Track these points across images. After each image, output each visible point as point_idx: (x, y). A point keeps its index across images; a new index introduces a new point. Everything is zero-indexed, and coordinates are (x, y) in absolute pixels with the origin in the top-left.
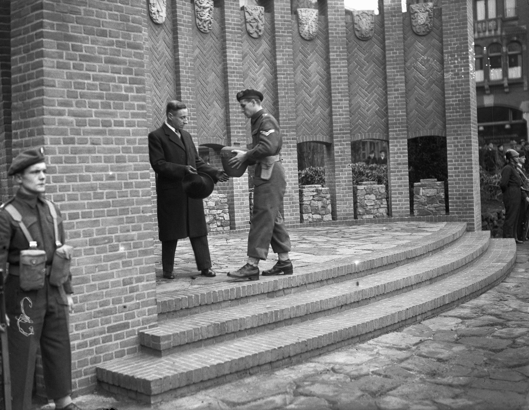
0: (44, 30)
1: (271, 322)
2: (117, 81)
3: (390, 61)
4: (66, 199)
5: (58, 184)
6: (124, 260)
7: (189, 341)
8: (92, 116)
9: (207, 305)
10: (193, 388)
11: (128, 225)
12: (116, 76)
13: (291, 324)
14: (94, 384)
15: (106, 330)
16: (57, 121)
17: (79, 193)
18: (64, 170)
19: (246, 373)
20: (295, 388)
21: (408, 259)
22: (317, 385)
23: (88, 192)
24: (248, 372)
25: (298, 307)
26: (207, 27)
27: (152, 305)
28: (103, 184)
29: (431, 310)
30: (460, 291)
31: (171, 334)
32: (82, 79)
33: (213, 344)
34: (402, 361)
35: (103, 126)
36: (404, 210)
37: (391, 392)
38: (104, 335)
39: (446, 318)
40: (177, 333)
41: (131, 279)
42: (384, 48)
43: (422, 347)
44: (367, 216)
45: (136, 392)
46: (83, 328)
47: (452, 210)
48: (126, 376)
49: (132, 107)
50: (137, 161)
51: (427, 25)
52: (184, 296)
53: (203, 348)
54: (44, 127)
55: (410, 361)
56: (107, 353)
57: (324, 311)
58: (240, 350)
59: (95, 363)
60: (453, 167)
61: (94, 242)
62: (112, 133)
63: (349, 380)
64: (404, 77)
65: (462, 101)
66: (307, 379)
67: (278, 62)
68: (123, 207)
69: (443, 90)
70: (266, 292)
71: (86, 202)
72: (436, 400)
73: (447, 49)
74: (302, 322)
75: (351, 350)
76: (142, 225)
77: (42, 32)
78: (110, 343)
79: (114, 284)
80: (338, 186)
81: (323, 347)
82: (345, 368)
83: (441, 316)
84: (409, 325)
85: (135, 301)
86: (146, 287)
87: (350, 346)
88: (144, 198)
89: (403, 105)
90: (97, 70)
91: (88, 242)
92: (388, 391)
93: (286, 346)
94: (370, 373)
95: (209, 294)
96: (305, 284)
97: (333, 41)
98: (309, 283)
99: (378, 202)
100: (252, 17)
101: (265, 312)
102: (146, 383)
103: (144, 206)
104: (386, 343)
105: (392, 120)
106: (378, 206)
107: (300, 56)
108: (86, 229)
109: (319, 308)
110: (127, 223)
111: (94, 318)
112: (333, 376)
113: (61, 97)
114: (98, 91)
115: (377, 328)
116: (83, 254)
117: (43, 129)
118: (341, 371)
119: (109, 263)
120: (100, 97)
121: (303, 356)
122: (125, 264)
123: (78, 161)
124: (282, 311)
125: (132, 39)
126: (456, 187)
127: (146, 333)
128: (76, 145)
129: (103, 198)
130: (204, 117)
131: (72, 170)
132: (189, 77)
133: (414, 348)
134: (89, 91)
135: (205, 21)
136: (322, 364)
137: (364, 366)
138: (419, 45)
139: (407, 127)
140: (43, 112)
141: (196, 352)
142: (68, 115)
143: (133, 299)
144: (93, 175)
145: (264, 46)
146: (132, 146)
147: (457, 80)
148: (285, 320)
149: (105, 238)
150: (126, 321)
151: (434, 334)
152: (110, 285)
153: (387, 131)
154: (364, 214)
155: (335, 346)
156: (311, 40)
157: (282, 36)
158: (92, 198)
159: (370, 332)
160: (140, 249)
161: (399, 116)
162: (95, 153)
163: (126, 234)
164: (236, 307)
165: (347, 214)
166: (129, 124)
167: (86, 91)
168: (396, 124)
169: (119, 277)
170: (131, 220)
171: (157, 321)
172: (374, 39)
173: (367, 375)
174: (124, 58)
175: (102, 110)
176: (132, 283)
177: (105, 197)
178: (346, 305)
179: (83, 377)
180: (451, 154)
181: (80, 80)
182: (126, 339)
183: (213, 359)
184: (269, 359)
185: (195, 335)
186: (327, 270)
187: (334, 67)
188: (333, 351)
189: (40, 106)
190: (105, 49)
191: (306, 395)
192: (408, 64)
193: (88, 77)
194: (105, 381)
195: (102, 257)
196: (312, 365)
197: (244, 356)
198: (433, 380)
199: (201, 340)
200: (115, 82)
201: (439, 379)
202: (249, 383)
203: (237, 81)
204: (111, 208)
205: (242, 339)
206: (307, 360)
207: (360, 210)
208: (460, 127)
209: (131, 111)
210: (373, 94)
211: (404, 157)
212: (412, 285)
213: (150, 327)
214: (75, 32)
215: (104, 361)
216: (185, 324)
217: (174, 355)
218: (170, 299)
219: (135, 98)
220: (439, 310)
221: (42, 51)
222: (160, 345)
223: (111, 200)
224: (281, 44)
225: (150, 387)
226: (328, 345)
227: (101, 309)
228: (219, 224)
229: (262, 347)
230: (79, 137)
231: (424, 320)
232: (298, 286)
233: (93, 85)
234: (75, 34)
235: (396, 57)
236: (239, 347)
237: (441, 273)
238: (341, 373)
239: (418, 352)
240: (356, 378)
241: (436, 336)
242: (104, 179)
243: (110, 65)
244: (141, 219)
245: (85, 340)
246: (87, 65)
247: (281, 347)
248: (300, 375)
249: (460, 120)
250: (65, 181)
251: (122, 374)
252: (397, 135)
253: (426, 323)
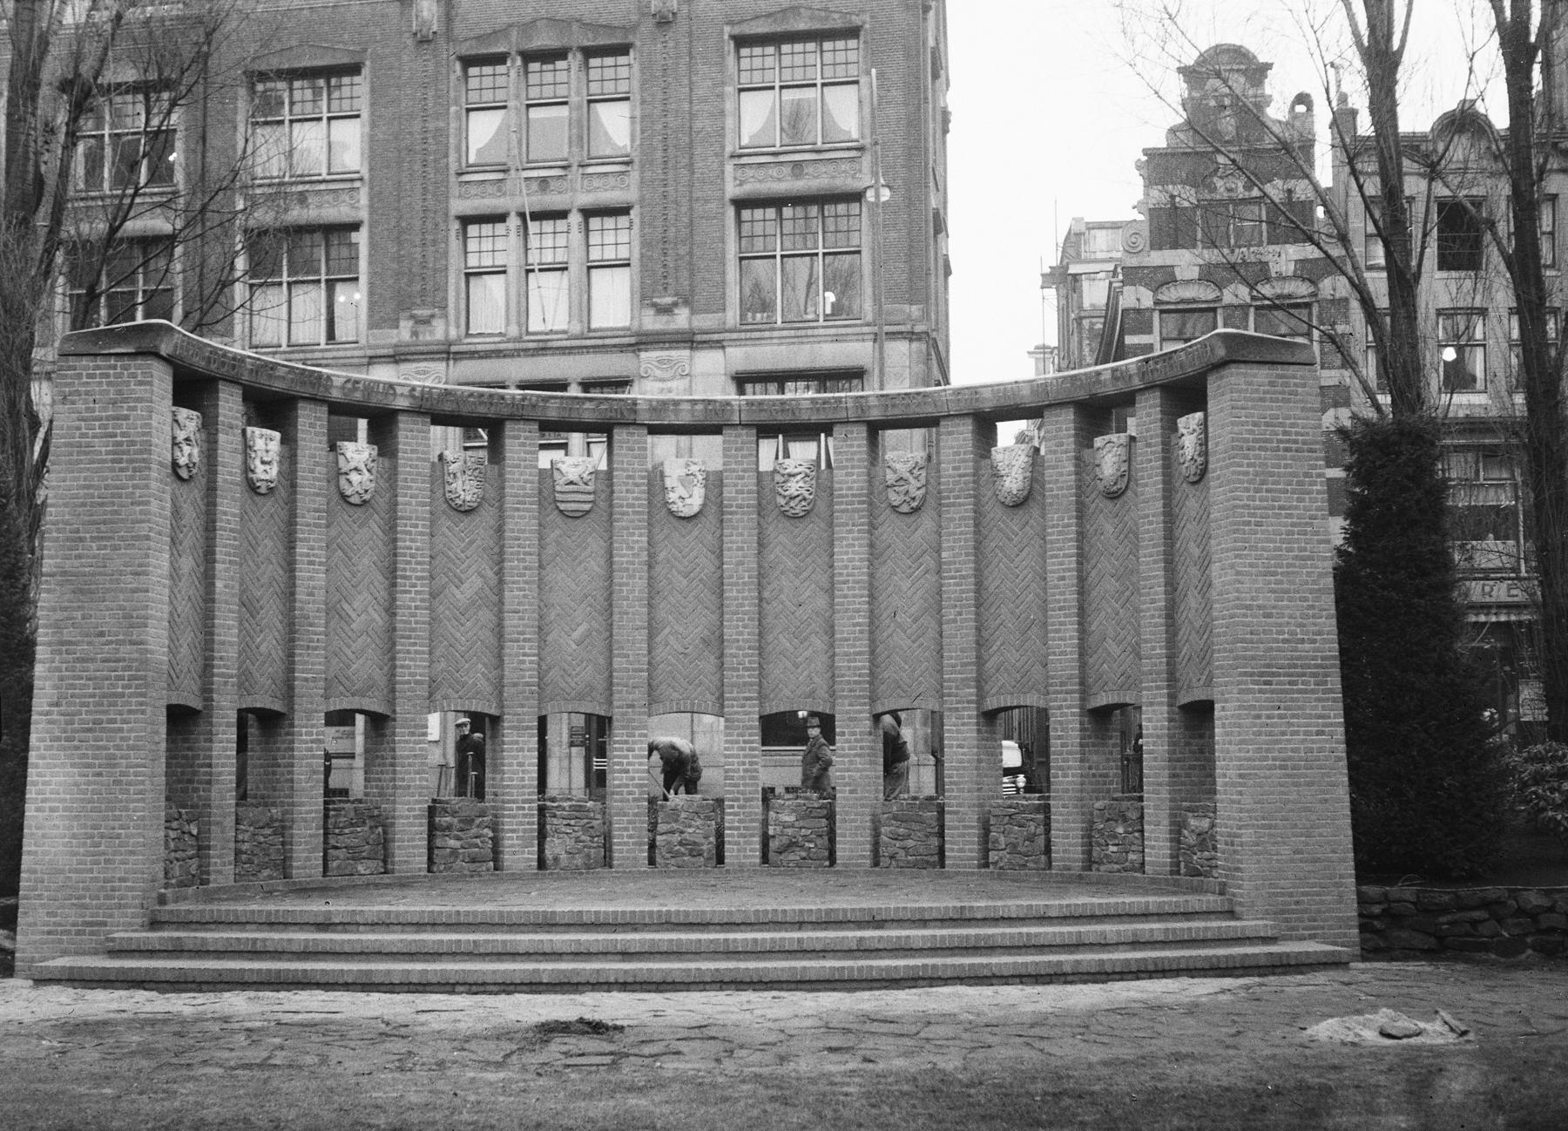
49: (130, 704)
62: (103, 730)
100: (895, 477)
135: (792, 498)
157: (953, 505)
224: (953, 519)
228: (804, 854)
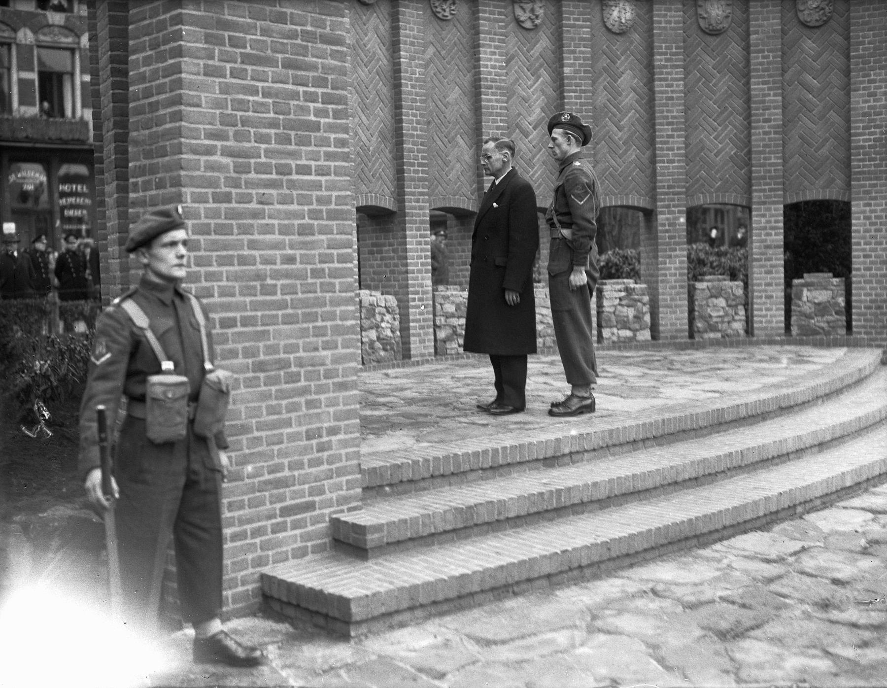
0: (184, 11)
1: (549, 508)
2: (302, 99)
3: (757, 70)
4: (216, 294)
5: (202, 270)
6: (309, 397)
7: (414, 536)
8: (260, 157)
9: (443, 476)
10: (419, 613)
11: (315, 339)
12: (301, 89)
13: (583, 513)
14: (256, 600)
15: (278, 512)
16: (202, 164)
17: (237, 285)
18: (214, 246)
19: (508, 591)
20: (589, 619)
21: (781, 409)
22: (626, 616)
23: (252, 283)
24: (511, 590)
25: (595, 484)
26: (448, 10)
27: (350, 473)
28: (277, 271)
29: (821, 497)
30: (872, 465)
31: (384, 522)
32: (245, 94)
33: (453, 541)
34: (770, 580)
35: (277, 173)
36: (774, 325)
37: (752, 633)
38: (274, 521)
39: (844, 511)
40: (394, 522)
41: (319, 429)
42: (747, 48)
43: (804, 557)
44: (712, 335)
45: (326, 616)
46: (241, 507)
47: (857, 326)
48: (311, 589)
49: (325, 142)
50: (332, 234)
51: (823, 9)
52: (406, 461)
53: (435, 547)
54: (183, 173)
55: (785, 581)
56: (279, 550)
57: (639, 492)
58: (497, 553)
59: (259, 565)
60: (862, 254)
61: (260, 367)
63: (680, 609)
64: (780, 98)
65: (880, 140)
66: (610, 606)
67: (567, 70)
68: (308, 310)
69: (848, 121)
70: (541, 457)
71: (248, 299)
72: (831, 650)
73: (857, 50)
74: (601, 509)
75: (685, 559)
76: (340, 339)
77: (181, 14)
78: (284, 534)
79: (292, 437)
80: (662, 281)
81: (637, 553)
82: (674, 588)
83: (837, 507)
84: (783, 520)
85: (325, 467)
86: (345, 444)
87: (682, 553)
88: (343, 294)
89: (776, 146)
90: (270, 80)
91: (251, 366)
92: (747, 630)
93: (574, 549)
94: (717, 599)
95: (447, 458)
96: (607, 446)
97: (660, 35)
98: (614, 445)
99: (731, 311)
101: (540, 491)
102: (343, 602)
103: (343, 308)
104: (744, 550)
105: (758, 171)
106: (730, 318)
107: (604, 62)
108: (247, 344)
109: (630, 486)
110: (315, 336)
111: (259, 491)
112: (653, 601)
113: (210, 124)
114: (272, 115)
115: (728, 523)
116: (242, 386)
117: (180, 176)
118: (667, 594)
119: (284, 402)
120: (273, 124)
121: (603, 566)
122: (310, 404)
123: (235, 231)
124: (569, 489)
125: (328, 28)
126: (865, 289)
127: (343, 519)
128: (234, 205)
129: (275, 294)
130: (440, 162)
131: (225, 247)
132: (417, 94)
133: (791, 559)
134: (256, 114)
136: (635, 581)
137: (705, 587)
138: (809, 45)
139: (784, 184)
140: (181, 148)
141: (424, 554)
142: (222, 155)
143: (322, 463)
144: (260, 256)
145: (543, 43)
146: (324, 208)
147: (872, 104)
148: (574, 505)
149: (278, 361)
150: (311, 499)
151: (825, 538)
152: (285, 438)
153: (749, 192)
154: (706, 331)
155: (656, 552)
156: (622, 33)
157: (574, 26)
158: (258, 293)
159: (717, 531)
160: (336, 380)
161: (771, 165)
162: (264, 218)
163: (313, 354)
164: (491, 481)
165: (677, 331)
166: (322, 171)
167: (250, 114)
168: (764, 178)
169: (300, 425)
170: (320, 332)
171: (362, 500)
172: (731, 33)
173: (712, 602)
174: (314, 59)
175: (277, 146)
176: (320, 436)
177: (279, 292)
178: (676, 483)
179: (240, 589)
180: (858, 231)
181: (241, 96)
182: (310, 528)
183: (453, 567)
184: (547, 569)
185: (424, 524)
186: (644, 424)
187: (660, 80)
188: (653, 560)
189: (175, 138)
190: (282, 43)
191: (609, 632)
192: (788, 76)
193: (254, 92)
194: (276, 596)
195: (273, 392)
196: (618, 582)
197: (504, 563)
198: (824, 615)
199: (433, 535)
200: (299, 100)
201: (835, 615)
202: (513, 609)
203: (497, 101)
204: (289, 311)
205: (499, 534)
206: (610, 574)
207: (699, 324)
208: (875, 185)
209: (325, 149)
210: (727, 127)
211: (776, 234)
212: (788, 454)
213: (349, 510)
214: (234, 16)
215: (274, 563)
216: (406, 507)
217: (388, 557)
218: (382, 464)
219: (331, 128)
220: (834, 497)
221: (180, 46)
222: (365, 540)
223: (288, 297)
224: (573, 39)
225: (350, 609)
226: (645, 550)
227: (271, 476)
229: (534, 550)
230: (238, 191)
231: (808, 513)
232: (594, 450)
233: (262, 104)
234: (235, 18)
235: (768, 63)
236: (496, 547)
237: (837, 435)
238: (665, 597)
239: (798, 567)
240: (692, 606)
241: (828, 541)
242: (278, 261)
243: (290, 72)
244: (337, 330)
245: (245, 527)
246: (253, 70)
247: (566, 551)
248: (598, 599)
249: (875, 172)
250: (215, 263)
251: (303, 586)
252: (766, 197)
253: (812, 517)
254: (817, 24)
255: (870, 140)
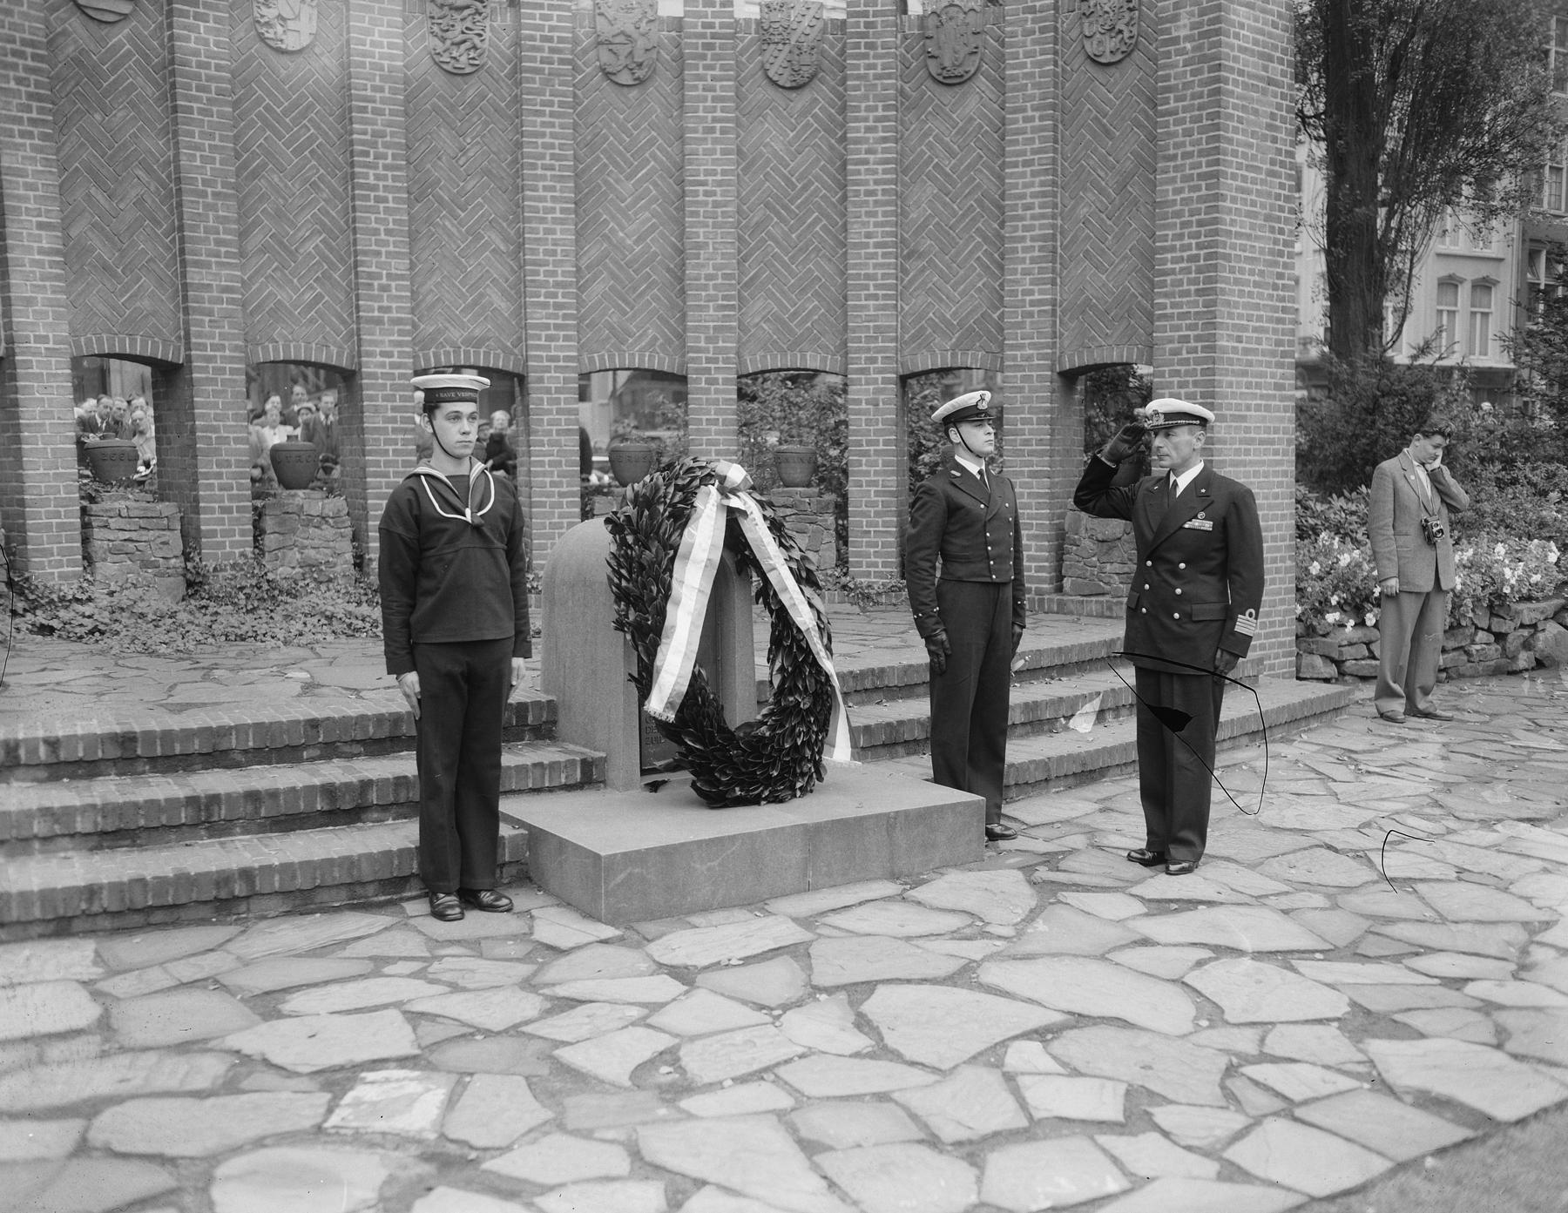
26: (463, 59)
51: (1120, 32)
254: (1119, 56)
255: (1182, 259)
